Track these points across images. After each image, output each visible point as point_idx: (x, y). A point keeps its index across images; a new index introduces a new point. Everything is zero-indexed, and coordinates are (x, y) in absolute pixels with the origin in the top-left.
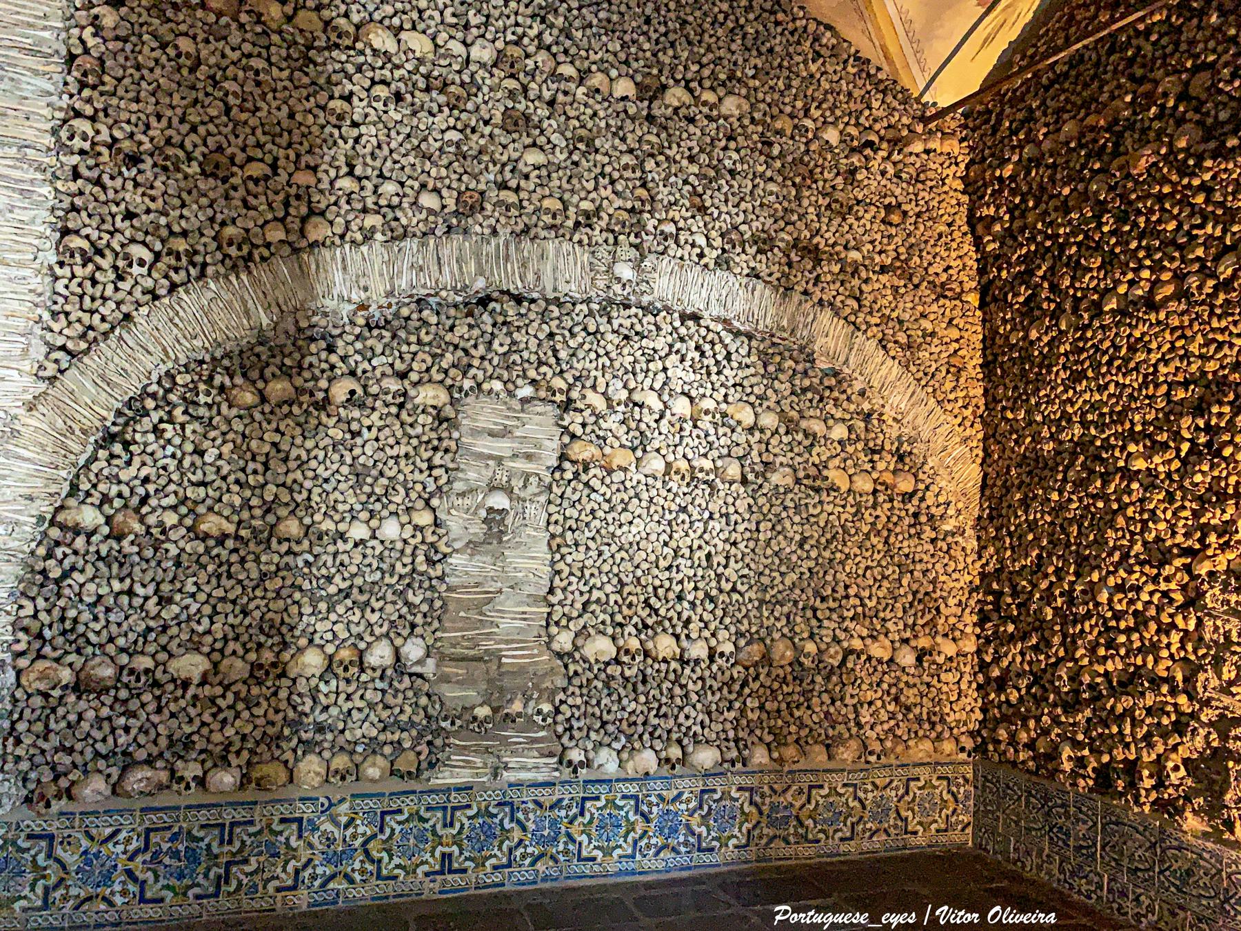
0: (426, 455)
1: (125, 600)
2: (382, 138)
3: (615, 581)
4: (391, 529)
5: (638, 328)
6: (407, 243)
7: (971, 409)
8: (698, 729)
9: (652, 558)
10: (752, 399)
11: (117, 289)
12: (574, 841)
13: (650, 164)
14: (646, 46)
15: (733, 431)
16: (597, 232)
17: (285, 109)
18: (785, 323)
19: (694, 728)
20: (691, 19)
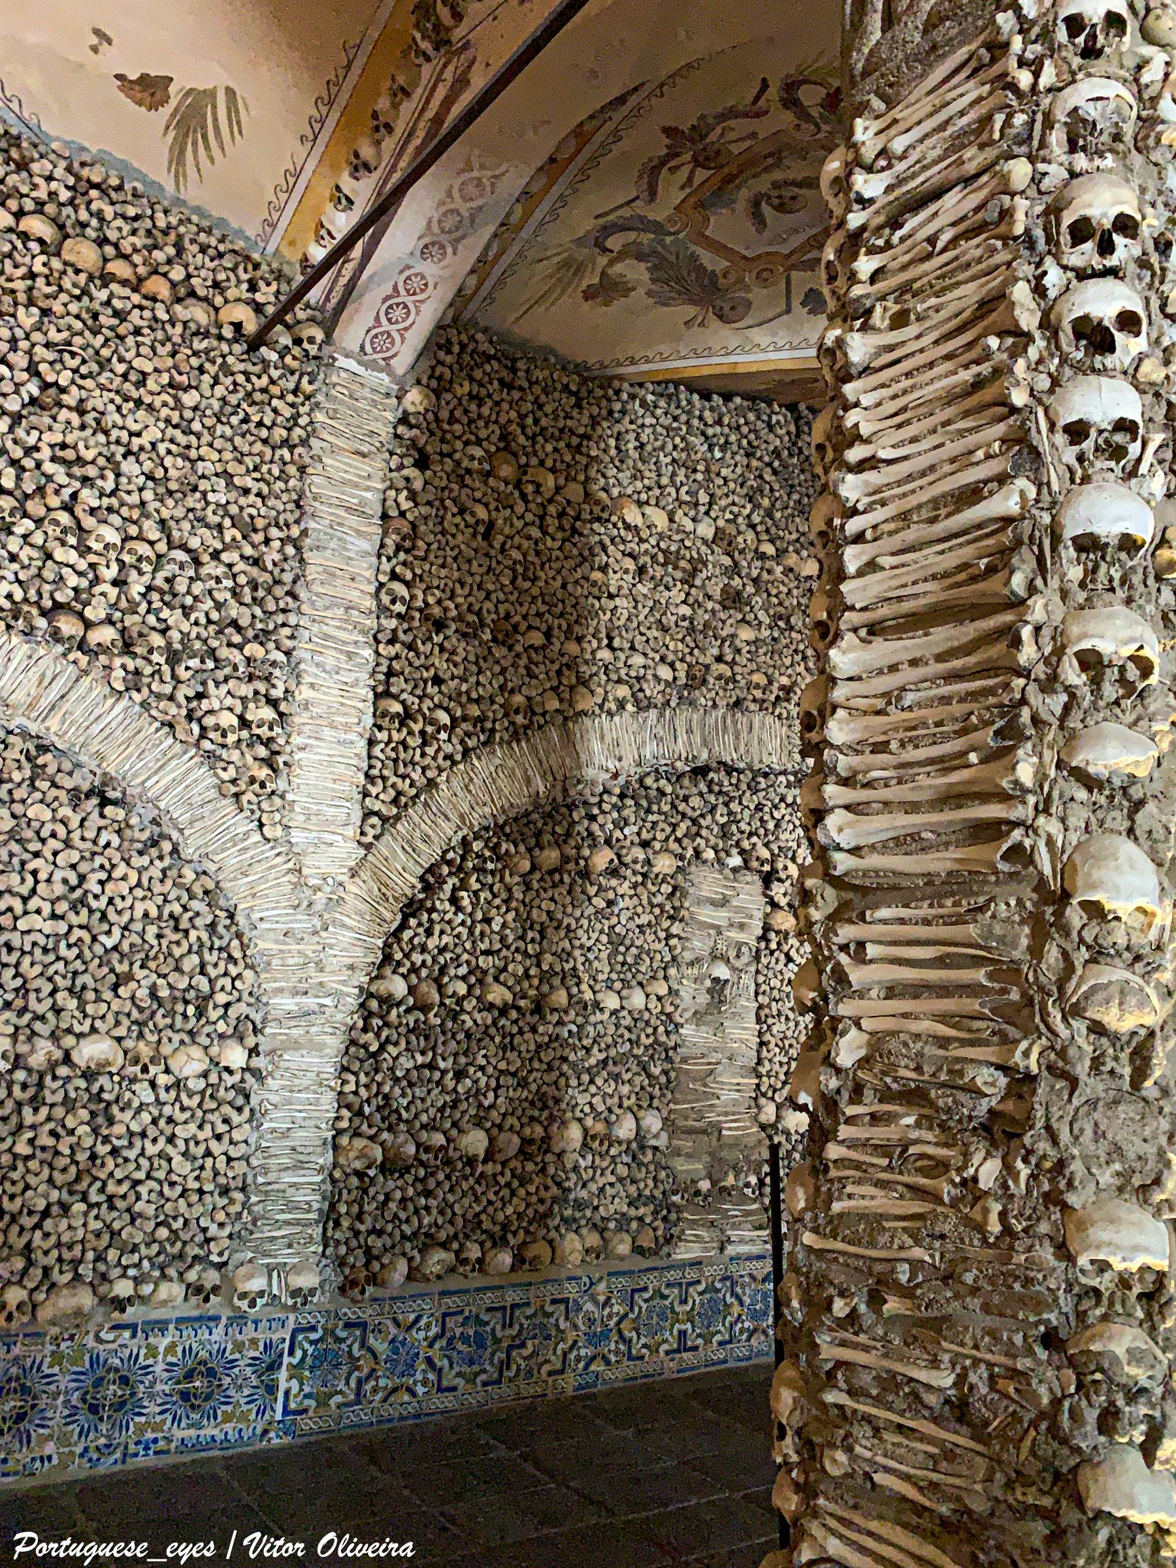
4: (637, 999)
11: (423, 755)
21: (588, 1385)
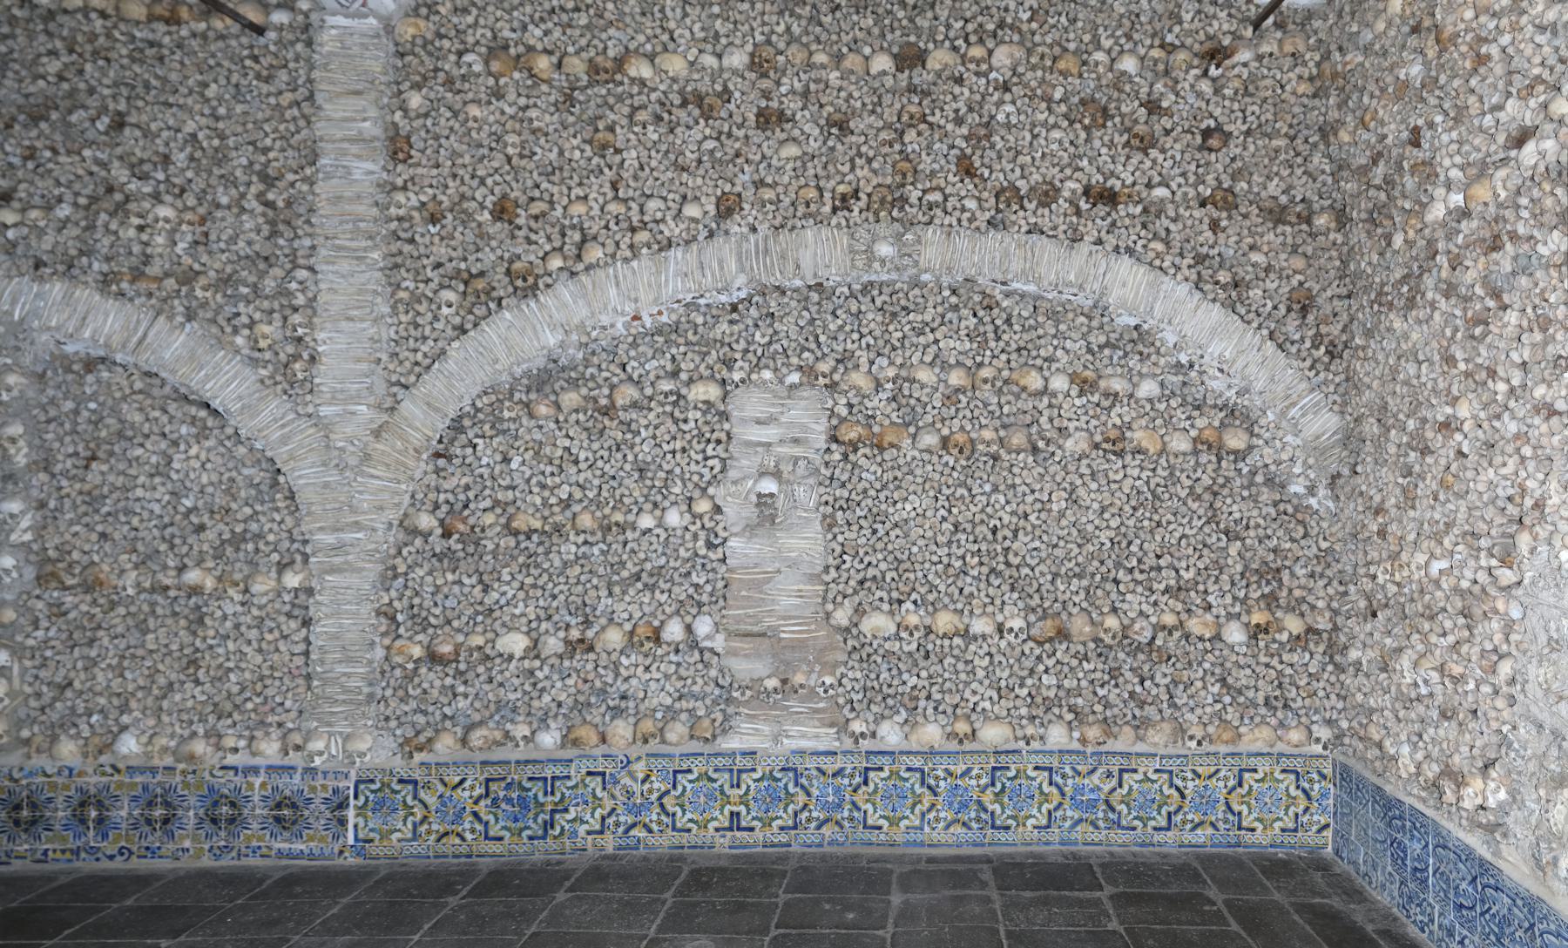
0: (699, 447)
1: (456, 589)
2: (644, 160)
3: (890, 558)
5: (903, 302)
6: (672, 252)
7: (1323, 349)
8: (987, 705)
9: (929, 534)
10: (1039, 362)
12: (859, 809)
13: (910, 135)
14: (901, 14)
15: (1018, 397)
16: (856, 213)
17: (556, 150)
19: (982, 705)
21: (628, 847)
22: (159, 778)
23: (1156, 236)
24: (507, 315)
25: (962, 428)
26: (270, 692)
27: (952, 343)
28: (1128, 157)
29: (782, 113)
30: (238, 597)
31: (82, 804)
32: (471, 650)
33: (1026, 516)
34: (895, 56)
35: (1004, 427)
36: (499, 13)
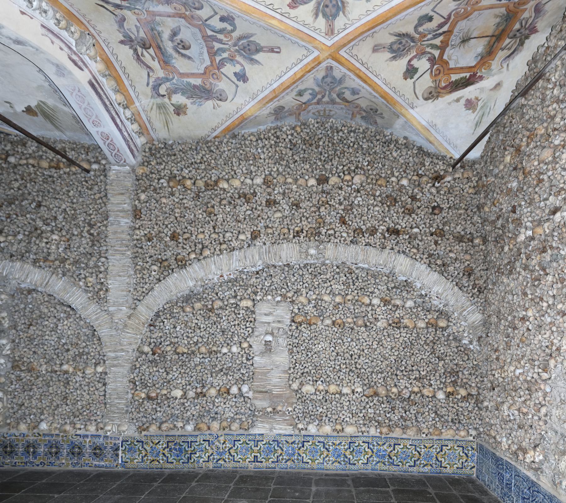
0: (244, 324)
1: (157, 373)
2: (225, 218)
5: (319, 271)
7: (476, 290)
8: (348, 419)
9: (327, 356)
10: (368, 293)
13: (322, 209)
14: (320, 163)
15: (361, 306)
18: (381, 262)
19: (346, 419)
20: (338, 148)
21: (217, 467)
22: (54, 438)
23: (414, 247)
24: (175, 275)
25: (340, 318)
26: (92, 409)
27: (337, 286)
28: (404, 217)
29: (275, 201)
30: (81, 375)
31: (28, 446)
32: (162, 396)
33: (363, 350)
34: (317, 180)
35: (356, 317)
36: (173, 164)
